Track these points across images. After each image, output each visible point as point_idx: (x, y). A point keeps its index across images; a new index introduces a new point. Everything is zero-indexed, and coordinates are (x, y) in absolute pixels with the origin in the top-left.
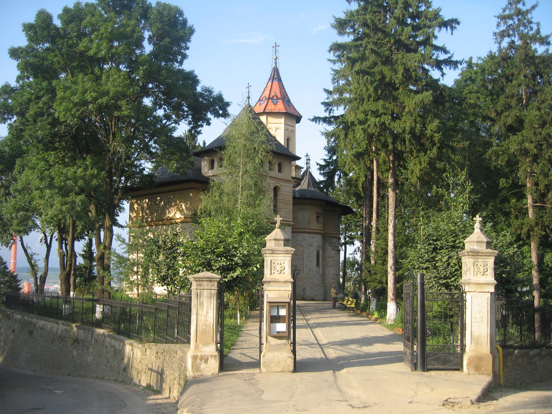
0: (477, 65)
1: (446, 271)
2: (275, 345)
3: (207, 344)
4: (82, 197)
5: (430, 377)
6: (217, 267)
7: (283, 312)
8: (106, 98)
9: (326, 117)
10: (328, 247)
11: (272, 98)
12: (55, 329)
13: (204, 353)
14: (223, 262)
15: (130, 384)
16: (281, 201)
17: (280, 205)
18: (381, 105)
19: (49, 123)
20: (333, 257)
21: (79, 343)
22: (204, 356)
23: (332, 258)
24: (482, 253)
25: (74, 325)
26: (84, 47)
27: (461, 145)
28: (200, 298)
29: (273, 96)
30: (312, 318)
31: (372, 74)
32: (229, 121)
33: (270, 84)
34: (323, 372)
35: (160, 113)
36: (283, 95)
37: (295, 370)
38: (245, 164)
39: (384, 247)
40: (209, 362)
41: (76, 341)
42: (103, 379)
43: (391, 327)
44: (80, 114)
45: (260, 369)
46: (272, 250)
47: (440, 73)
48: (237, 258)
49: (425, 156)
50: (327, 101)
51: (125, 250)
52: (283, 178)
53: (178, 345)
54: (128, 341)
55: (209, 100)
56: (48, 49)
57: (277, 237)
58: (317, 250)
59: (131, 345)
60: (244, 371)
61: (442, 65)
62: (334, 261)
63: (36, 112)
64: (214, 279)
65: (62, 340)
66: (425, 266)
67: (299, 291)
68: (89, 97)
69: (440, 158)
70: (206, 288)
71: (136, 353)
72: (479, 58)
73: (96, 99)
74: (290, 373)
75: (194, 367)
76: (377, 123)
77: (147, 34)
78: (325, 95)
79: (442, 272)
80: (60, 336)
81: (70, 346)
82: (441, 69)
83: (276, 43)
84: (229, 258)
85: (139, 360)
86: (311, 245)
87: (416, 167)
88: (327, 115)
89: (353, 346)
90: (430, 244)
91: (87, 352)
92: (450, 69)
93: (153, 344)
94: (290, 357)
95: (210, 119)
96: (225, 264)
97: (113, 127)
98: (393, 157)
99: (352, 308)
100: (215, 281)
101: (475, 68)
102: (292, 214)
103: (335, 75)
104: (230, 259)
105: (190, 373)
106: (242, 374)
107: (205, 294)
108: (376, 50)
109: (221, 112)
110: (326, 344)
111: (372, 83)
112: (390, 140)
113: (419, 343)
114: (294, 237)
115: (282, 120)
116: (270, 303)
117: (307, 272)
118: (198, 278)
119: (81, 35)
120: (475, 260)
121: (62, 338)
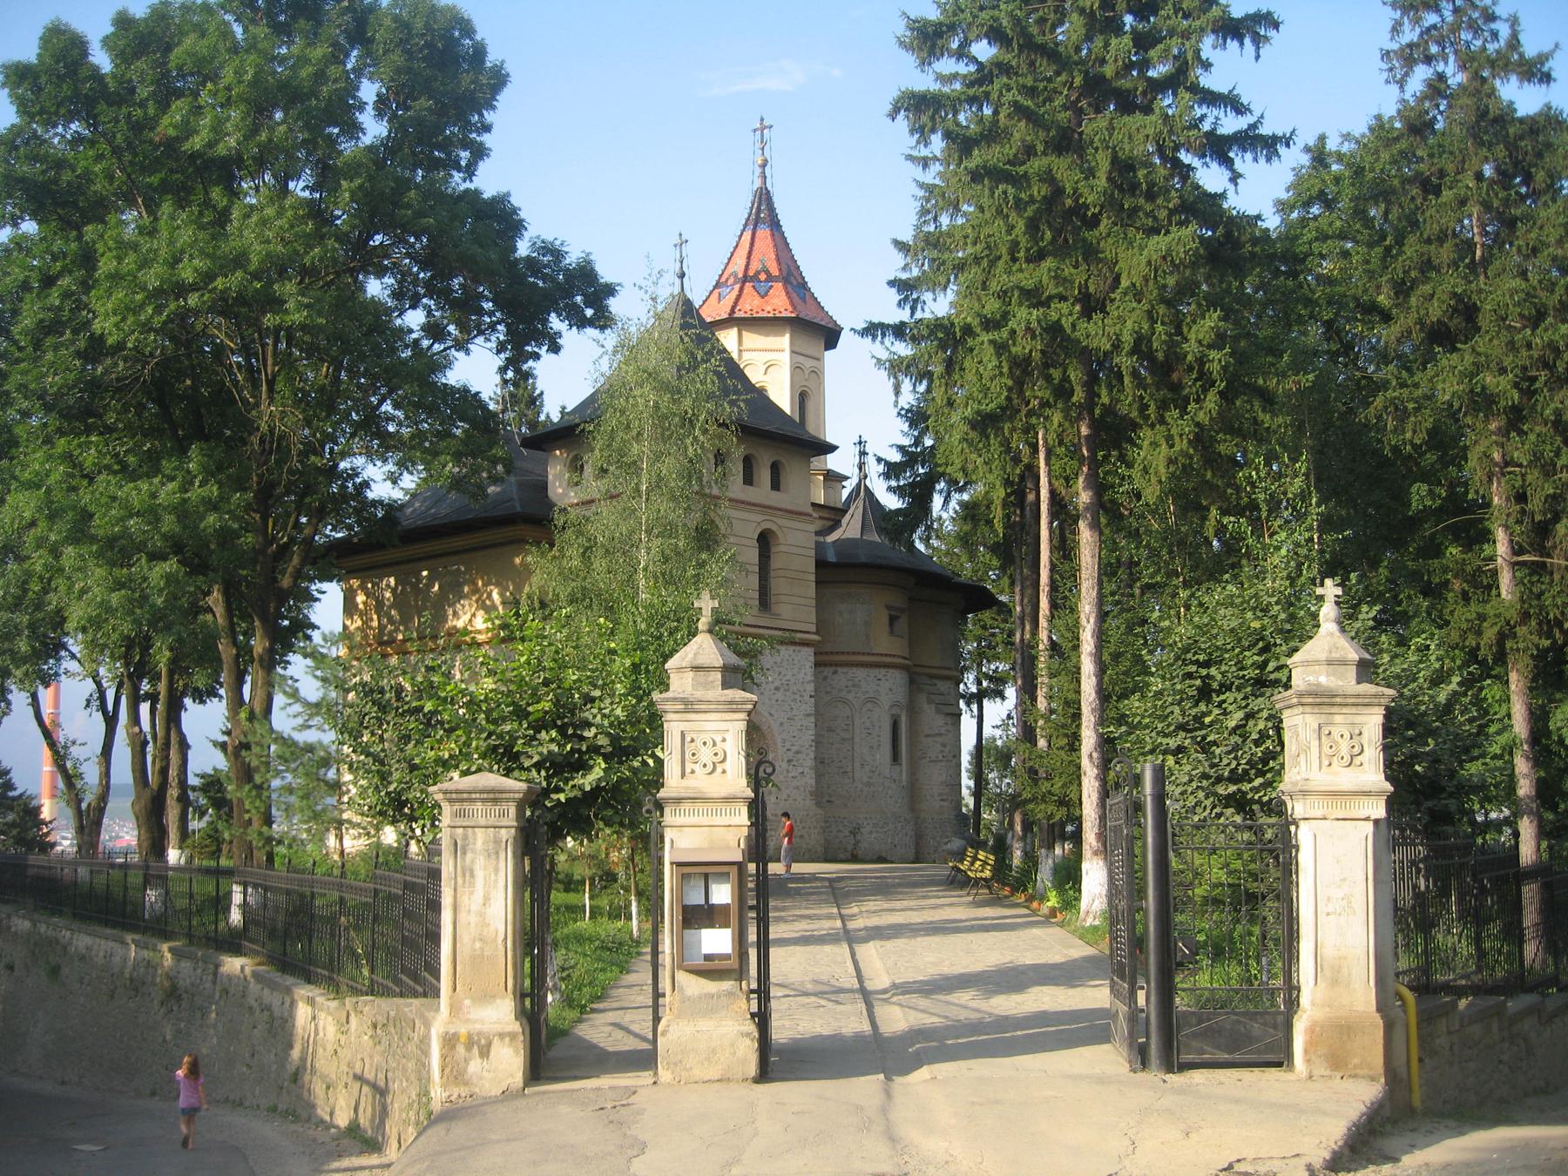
0: (1340, 157)
1: (1236, 758)
2: (700, 998)
3: (486, 997)
4: (171, 565)
5: (1181, 1091)
6: (535, 760)
7: (722, 894)
8: (239, 274)
9: (903, 324)
10: (926, 706)
11: (755, 278)
12: (117, 959)
13: (478, 1027)
14: (548, 743)
15: (309, 1120)
16: (781, 573)
17: (778, 585)
18: (1049, 270)
19: (78, 354)
20: (940, 735)
21: (179, 998)
22: (479, 1034)
23: (937, 739)
24: (1345, 696)
25: (165, 947)
26: (175, 127)
27: (1290, 384)
28: (464, 853)
29: (758, 273)
30: (861, 912)
31: (1019, 181)
32: (610, 338)
33: (747, 236)
34: (854, 1080)
35: (414, 319)
36: (784, 267)
37: (765, 1073)
38: (658, 457)
39: (1071, 696)
40: (492, 1053)
41: (173, 993)
42: (241, 1104)
43: (1087, 935)
44: (165, 323)
45: (656, 1074)
46: (685, 701)
47: (1227, 174)
48: (594, 730)
49: (1181, 417)
50: (904, 276)
51: (300, 721)
53: (415, 1002)
54: (302, 992)
55: (553, 280)
56: (78, 140)
57: (701, 661)
58: (893, 715)
59: (311, 1002)
60: (605, 1081)
61: (1230, 149)
62: (944, 745)
63: (42, 321)
64: (504, 796)
65: (136, 990)
66: (1173, 743)
68: (187, 274)
69: (1228, 423)
70: (482, 821)
71: (324, 1028)
72: (1347, 137)
73: (209, 277)
74: (746, 1084)
75: (447, 1071)
76: (1034, 325)
77: (369, 91)
78: (899, 259)
79: (1225, 761)
80: (131, 980)
81: (157, 1008)
82: (1227, 162)
83: (762, 120)
84: (570, 731)
85: (330, 1049)
86: (873, 701)
87: (1156, 453)
88: (904, 315)
89: (965, 997)
90: (1189, 676)
91: (201, 1026)
92: (1255, 160)
93: (370, 998)
94: (748, 1035)
95: (559, 334)
96: (556, 749)
97: (270, 362)
98: (1089, 427)
99: (985, 880)
100: (508, 800)
101: (1335, 167)
102: (813, 610)
103: (928, 201)
104: (574, 735)
105: (438, 1094)
106: (598, 1089)
107: (479, 843)
108: (1028, 108)
109: (589, 312)
110: (885, 991)
111: (1019, 205)
112: (1075, 375)
113: (1153, 984)
114: (825, 678)
115: (784, 341)
116: (679, 864)
117: (865, 779)
118: (457, 792)
119: (166, 95)
120: (1323, 719)
121: (137, 986)
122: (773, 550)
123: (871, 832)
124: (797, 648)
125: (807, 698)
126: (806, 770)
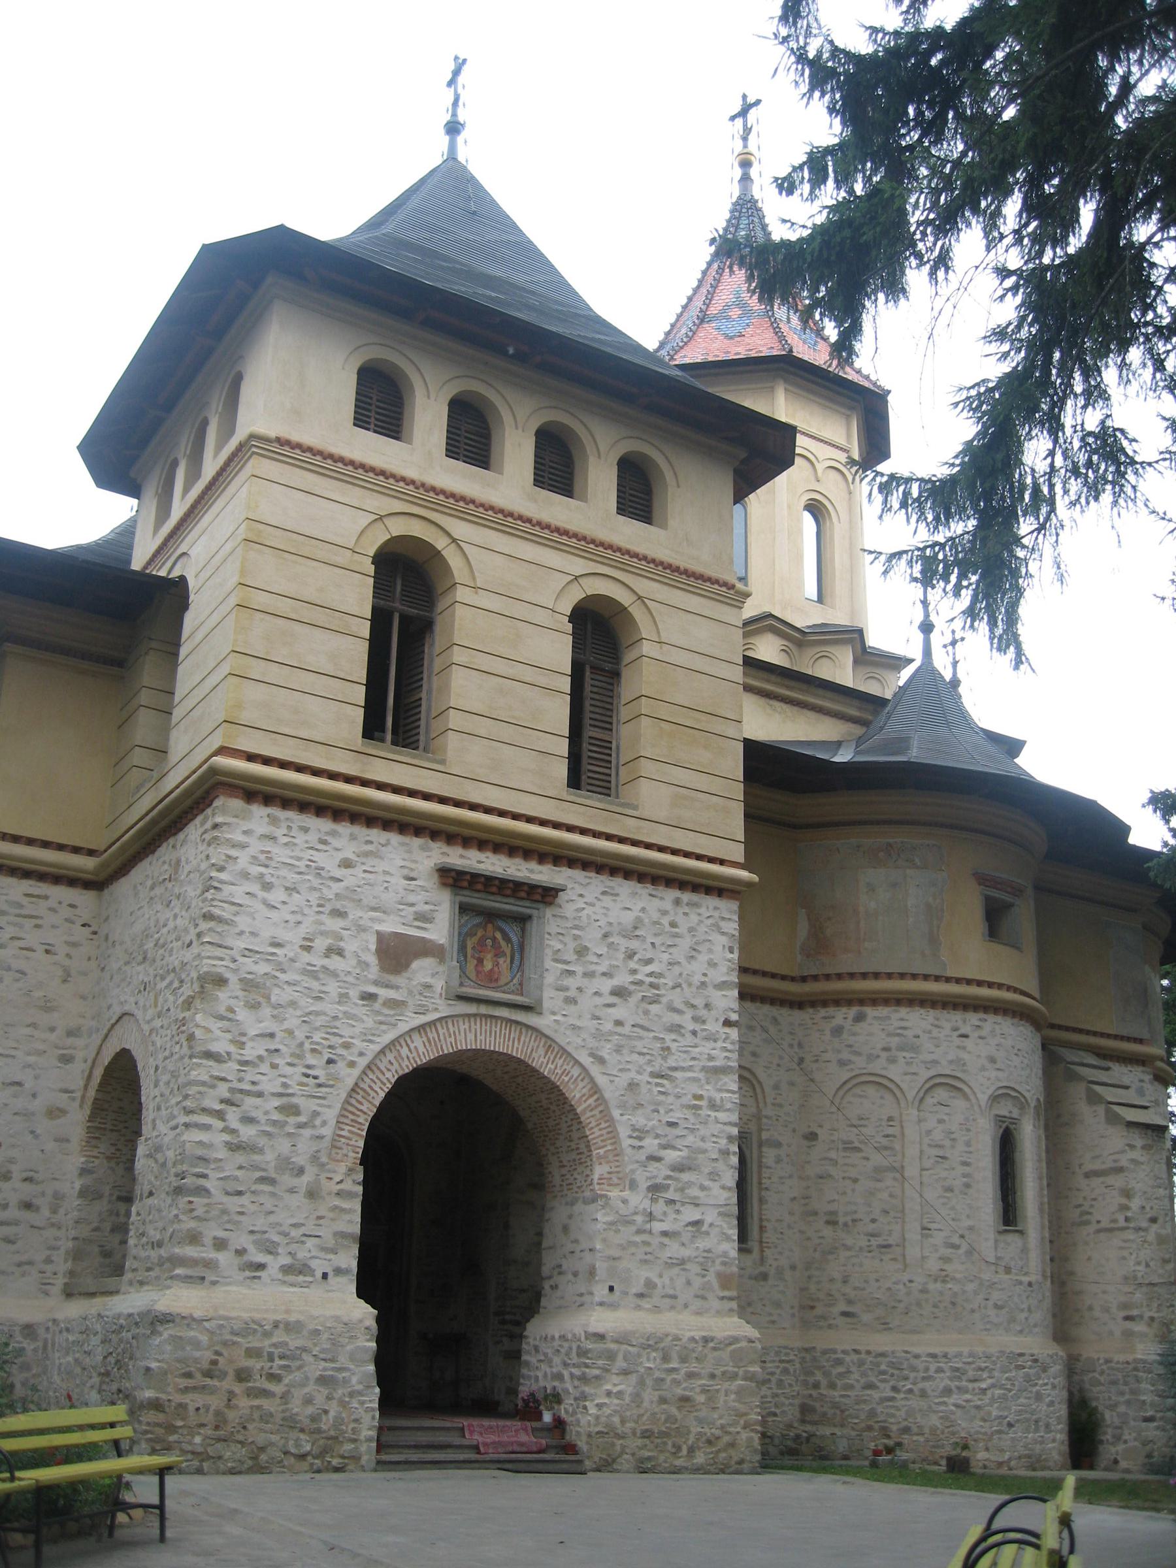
11: (723, 315)
20: (1120, 1170)
23: (1110, 1180)
33: (713, 272)
58: (999, 1119)
67: (876, 1395)
114: (838, 1031)
117: (933, 1265)
122: (628, 657)
123: (947, 1391)
124: (686, 896)
125: (714, 1026)
126: (710, 1216)
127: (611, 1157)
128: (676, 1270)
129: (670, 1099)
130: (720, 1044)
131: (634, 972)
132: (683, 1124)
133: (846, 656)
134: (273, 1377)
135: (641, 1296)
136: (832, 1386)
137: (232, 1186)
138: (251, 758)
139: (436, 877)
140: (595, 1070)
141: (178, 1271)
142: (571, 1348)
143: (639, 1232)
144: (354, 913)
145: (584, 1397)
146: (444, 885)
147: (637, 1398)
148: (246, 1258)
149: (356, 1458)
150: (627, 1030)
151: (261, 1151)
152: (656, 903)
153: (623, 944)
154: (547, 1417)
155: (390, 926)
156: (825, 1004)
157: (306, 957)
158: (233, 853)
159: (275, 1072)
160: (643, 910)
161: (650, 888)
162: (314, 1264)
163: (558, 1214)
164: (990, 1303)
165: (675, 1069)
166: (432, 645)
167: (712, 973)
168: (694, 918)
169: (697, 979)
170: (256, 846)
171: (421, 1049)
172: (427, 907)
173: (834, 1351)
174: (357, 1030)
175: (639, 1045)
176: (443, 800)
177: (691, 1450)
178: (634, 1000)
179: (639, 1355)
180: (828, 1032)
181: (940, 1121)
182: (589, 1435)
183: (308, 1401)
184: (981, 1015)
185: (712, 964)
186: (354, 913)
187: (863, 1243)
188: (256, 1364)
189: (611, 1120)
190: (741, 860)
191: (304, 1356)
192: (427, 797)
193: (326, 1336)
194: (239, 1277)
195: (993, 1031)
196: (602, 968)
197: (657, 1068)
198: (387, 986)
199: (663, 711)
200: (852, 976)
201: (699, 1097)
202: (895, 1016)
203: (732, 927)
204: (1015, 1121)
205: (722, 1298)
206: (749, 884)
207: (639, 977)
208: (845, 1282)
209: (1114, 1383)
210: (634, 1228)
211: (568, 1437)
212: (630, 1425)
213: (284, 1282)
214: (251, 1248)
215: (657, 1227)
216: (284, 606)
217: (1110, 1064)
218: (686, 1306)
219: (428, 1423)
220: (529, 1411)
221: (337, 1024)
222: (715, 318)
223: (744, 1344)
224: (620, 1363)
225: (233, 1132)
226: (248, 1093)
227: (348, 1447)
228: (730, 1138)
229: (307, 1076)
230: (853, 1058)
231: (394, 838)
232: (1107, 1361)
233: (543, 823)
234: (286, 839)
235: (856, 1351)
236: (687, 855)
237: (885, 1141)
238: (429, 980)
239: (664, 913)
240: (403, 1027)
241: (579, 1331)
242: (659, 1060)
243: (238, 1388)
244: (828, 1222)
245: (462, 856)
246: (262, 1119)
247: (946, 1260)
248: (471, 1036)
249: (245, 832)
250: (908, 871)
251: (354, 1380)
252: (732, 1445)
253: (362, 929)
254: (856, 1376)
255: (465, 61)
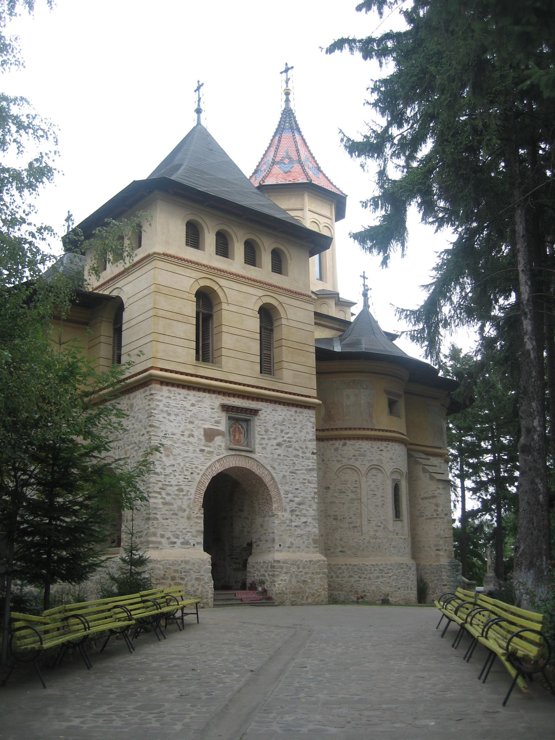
10: (421, 475)
11: (281, 162)
23: (431, 500)
52: (285, 286)
58: (394, 480)
67: (353, 580)
86: (377, 468)
102: (314, 378)
114: (336, 449)
117: (372, 533)
122: (276, 324)
123: (378, 577)
124: (299, 410)
125: (309, 455)
126: (310, 520)
127: (278, 501)
128: (299, 538)
129: (296, 480)
130: (311, 461)
131: (283, 437)
132: (300, 489)
133: (332, 303)
134: (182, 579)
135: (289, 547)
136: (337, 577)
137: (165, 517)
138: (161, 370)
139: (221, 408)
140: (272, 472)
141: (150, 546)
142: (268, 566)
143: (288, 526)
144: (196, 422)
145: (274, 581)
146: (223, 410)
147: (290, 580)
148: (170, 540)
149: (208, 604)
150: (281, 457)
151: (172, 504)
152: (289, 413)
153: (280, 427)
154: (260, 589)
155: (208, 426)
156: (331, 439)
157: (182, 438)
158: (158, 403)
159: (175, 478)
160: (285, 415)
161: (287, 408)
162: (191, 541)
163: (259, 521)
164: (391, 546)
165: (297, 470)
166: (212, 324)
167: (307, 436)
168: (301, 417)
169: (303, 438)
170: (165, 401)
171: (219, 467)
172: (219, 418)
173: (338, 565)
174: (199, 462)
175: (286, 462)
176: (221, 381)
177: (307, 598)
178: (283, 447)
179: (290, 567)
180: (333, 450)
181: (374, 481)
182: (276, 594)
183: (193, 586)
184: (388, 443)
185: (307, 433)
186: (196, 422)
187: (347, 526)
188: (177, 575)
189: (278, 489)
190: (316, 396)
191: (191, 571)
192: (216, 380)
193: (197, 565)
194: (169, 546)
195: (391, 448)
196: (273, 437)
197: (291, 470)
198: (208, 447)
199: (290, 344)
200: (341, 429)
201: (304, 479)
202: (357, 444)
203: (313, 420)
204: (399, 481)
205: (314, 547)
206: (319, 405)
207: (285, 439)
208: (341, 540)
209: (433, 573)
210: (286, 525)
211: (268, 595)
212: (288, 590)
213: (182, 548)
214: (171, 537)
215: (293, 524)
216: (169, 315)
217: (430, 457)
218: (303, 550)
219: (224, 592)
220: (253, 587)
221: (193, 460)
222: (278, 163)
223: (322, 562)
224: (285, 570)
225: (164, 498)
226: (168, 485)
227: (205, 600)
228: (315, 493)
229: (185, 478)
230: (343, 459)
231: (207, 395)
232: (430, 565)
233: (253, 386)
234: (174, 398)
235: (346, 565)
236: (298, 395)
237: (354, 489)
238: (220, 444)
239: (292, 416)
240: (213, 460)
241: (271, 560)
242: (292, 467)
243: (172, 583)
244: (334, 519)
245: (228, 400)
246: (172, 493)
247: (376, 531)
248: (234, 462)
249: (161, 396)
250: (362, 390)
251: (206, 579)
252: (319, 596)
253: (199, 427)
254: (346, 573)
255: (203, 84)
